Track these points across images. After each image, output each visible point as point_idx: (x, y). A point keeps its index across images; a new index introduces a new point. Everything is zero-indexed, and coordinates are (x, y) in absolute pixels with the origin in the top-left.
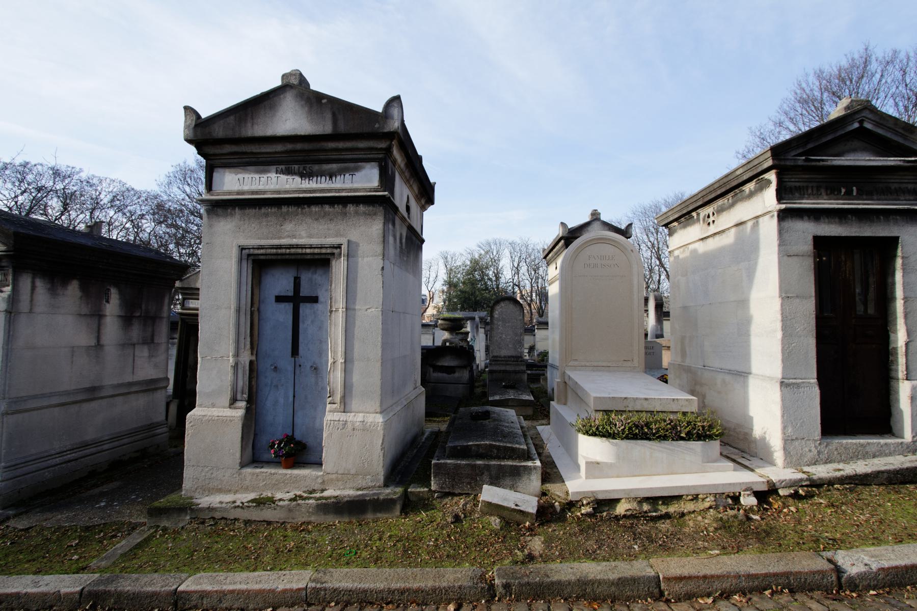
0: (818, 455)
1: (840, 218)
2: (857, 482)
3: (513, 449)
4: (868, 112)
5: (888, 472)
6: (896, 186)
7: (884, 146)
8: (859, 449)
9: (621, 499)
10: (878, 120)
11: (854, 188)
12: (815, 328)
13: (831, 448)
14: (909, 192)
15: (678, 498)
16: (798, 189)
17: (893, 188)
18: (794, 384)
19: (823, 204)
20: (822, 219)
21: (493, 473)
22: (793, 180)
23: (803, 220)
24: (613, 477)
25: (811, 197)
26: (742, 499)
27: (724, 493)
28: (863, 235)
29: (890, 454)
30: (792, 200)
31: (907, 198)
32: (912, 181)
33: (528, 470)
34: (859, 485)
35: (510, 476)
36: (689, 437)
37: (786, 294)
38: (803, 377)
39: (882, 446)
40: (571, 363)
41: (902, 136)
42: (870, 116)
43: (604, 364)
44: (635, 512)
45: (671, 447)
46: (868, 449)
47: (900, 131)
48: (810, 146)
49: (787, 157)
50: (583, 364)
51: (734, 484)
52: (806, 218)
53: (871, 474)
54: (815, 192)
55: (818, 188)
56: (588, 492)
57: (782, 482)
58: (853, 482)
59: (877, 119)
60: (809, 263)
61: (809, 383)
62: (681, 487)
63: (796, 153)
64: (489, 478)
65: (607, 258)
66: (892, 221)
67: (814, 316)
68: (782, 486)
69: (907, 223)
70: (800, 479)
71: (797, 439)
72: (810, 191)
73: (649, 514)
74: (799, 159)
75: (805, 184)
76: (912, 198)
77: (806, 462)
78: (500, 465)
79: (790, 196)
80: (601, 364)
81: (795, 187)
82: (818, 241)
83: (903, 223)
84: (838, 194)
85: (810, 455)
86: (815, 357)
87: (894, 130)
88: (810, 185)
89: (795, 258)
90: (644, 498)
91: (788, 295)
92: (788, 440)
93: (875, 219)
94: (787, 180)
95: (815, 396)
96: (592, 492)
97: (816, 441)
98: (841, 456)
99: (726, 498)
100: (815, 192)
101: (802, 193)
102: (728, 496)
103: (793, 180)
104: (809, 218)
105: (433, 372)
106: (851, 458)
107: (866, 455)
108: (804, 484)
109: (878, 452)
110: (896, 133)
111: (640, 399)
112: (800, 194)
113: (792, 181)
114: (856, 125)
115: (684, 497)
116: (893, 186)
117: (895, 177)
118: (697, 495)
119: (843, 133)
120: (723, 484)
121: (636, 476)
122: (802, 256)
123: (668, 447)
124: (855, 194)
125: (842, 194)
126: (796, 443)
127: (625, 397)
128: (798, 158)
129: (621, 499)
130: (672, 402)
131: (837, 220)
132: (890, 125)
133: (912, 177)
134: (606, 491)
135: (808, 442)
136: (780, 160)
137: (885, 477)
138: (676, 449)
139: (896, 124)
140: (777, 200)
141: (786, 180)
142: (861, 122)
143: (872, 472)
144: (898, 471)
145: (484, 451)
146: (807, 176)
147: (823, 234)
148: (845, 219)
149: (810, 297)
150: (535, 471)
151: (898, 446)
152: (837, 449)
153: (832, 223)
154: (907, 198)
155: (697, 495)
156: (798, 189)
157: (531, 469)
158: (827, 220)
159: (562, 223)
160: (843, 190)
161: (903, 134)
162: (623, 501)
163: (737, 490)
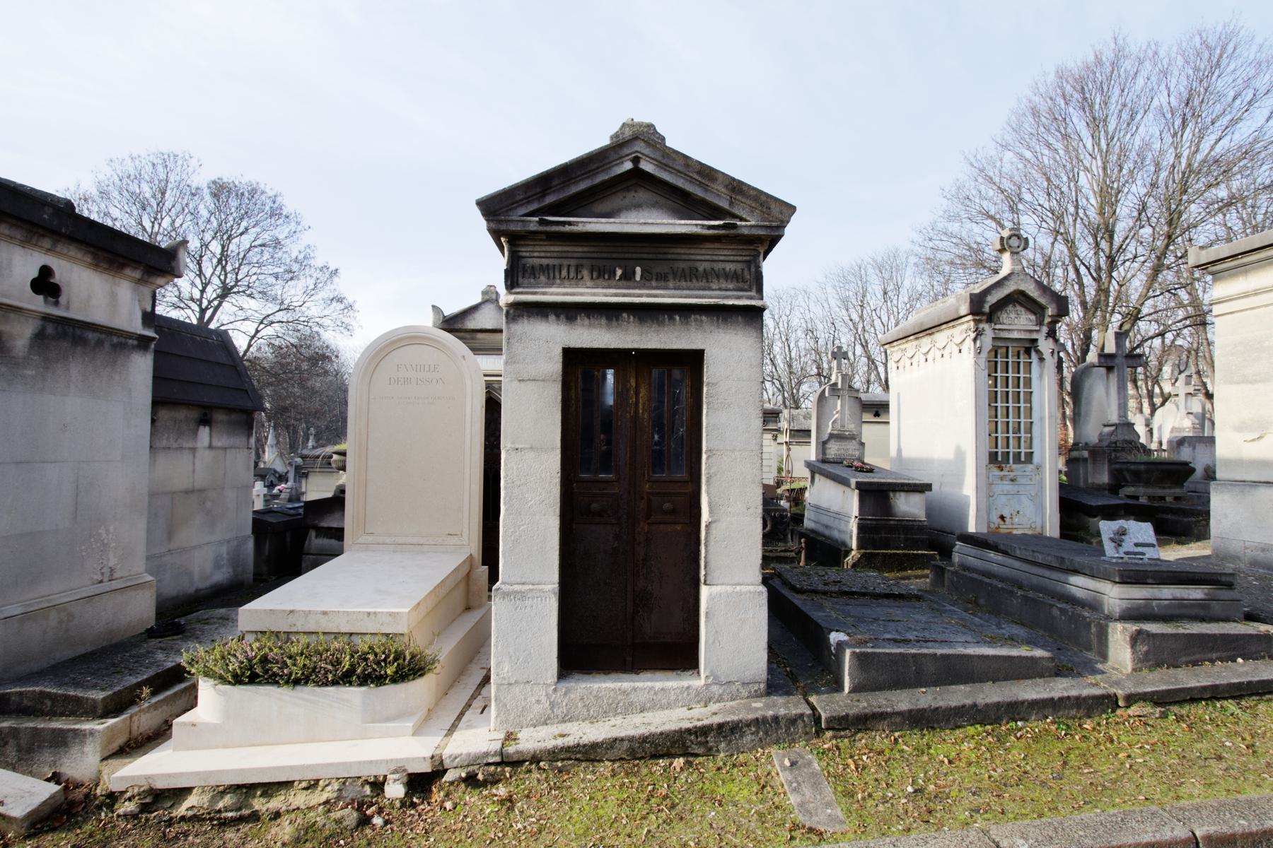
0: (552, 709)
1: (609, 319)
2: (578, 756)
3: (78, 700)
4: (642, 144)
5: (631, 739)
6: (707, 265)
7: (685, 203)
8: (620, 697)
9: (194, 788)
10: (660, 159)
11: (638, 270)
12: (559, 500)
13: (572, 696)
14: (728, 276)
15: (287, 785)
16: (545, 269)
17: (701, 269)
18: (517, 592)
19: (582, 294)
20: (579, 320)
21: (24, 742)
22: (536, 254)
23: (547, 321)
24: (217, 747)
25: (566, 283)
26: (386, 788)
27: (360, 777)
28: (646, 347)
29: (669, 706)
30: (535, 287)
31: (724, 286)
32: (732, 258)
33: (80, 736)
34: (582, 761)
35: (51, 747)
36: (346, 678)
37: (513, 443)
38: (536, 580)
39: (655, 694)
40: (363, 539)
41: (700, 184)
42: (647, 151)
43: (415, 541)
44: (201, 812)
45: (313, 698)
46: (633, 697)
47: (695, 176)
48: (550, 199)
49: (510, 218)
50: (380, 540)
51: (377, 762)
52: (552, 317)
53: (602, 743)
54: (572, 275)
55: (578, 269)
56: (139, 777)
57: (456, 758)
58: (573, 757)
59: (658, 156)
60: (554, 392)
61: (541, 591)
62: (292, 768)
63: (527, 211)
64: (17, 751)
65: (427, 369)
66: (693, 324)
67: (558, 480)
68: (455, 765)
69: (718, 327)
70: (484, 753)
71: (516, 682)
72: (564, 273)
73: (223, 815)
74: (530, 221)
75: (556, 262)
76: (731, 286)
77: (531, 720)
78: (36, 729)
79: (532, 280)
80: (410, 540)
81: (541, 265)
82: (572, 357)
83: (712, 328)
84: (609, 279)
85: (538, 709)
86: (558, 547)
87: (685, 175)
88: (566, 262)
89: (530, 384)
90: (232, 786)
91: (517, 447)
92: (504, 684)
93: (667, 320)
94: (528, 254)
95: (551, 611)
96: (147, 778)
97: (548, 685)
98: (588, 710)
99: (363, 786)
100: (572, 275)
101: (552, 276)
102: (367, 782)
103: (536, 254)
104: (558, 316)
105: (316, 537)
106: (605, 712)
107: (612, 710)
108: (491, 761)
109: (649, 702)
110: (692, 180)
111: (316, 613)
112: (549, 278)
113: (535, 255)
114: (628, 166)
115: (296, 784)
116: (701, 267)
117: (703, 251)
118: (318, 781)
119: (607, 178)
120: (360, 763)
121: (253, 745)
122: (543, 380)
123: (306, 696)
124: (638, 278)
125: (617, 278)
126: (516, 690)
127: (292, 608)
128: (529, 218)
129: (194, 788)
130: (366, 617)
131: (603, 321)
132: (677, 167)
133: (747, 253)
134: (169, 775)
135: (535, 688)
136: (499, 222)
137: (625, 748)
138: (321, 700)
139: (687, 166)
140: (507, 288)
141: (524, 254)
142: (636, 160)
143: (605, 739)
144: (647, 737)
145: (29, 704)
146: (557, 249)
147: (578, 345)
148: (617, 320)
149: (553, 449)
150: (91, 738)
151: (682, 693)
152: (582, 699)
153: (595, 327)
154: (724, 286)
155: (318, 781)
156: (545, 269)
157: (85, 735)
158: (586, 322)
159: (433, 306)
160: (619, 272)
161: (700, 182)
162: (195, 791)
163: (381, 772)
